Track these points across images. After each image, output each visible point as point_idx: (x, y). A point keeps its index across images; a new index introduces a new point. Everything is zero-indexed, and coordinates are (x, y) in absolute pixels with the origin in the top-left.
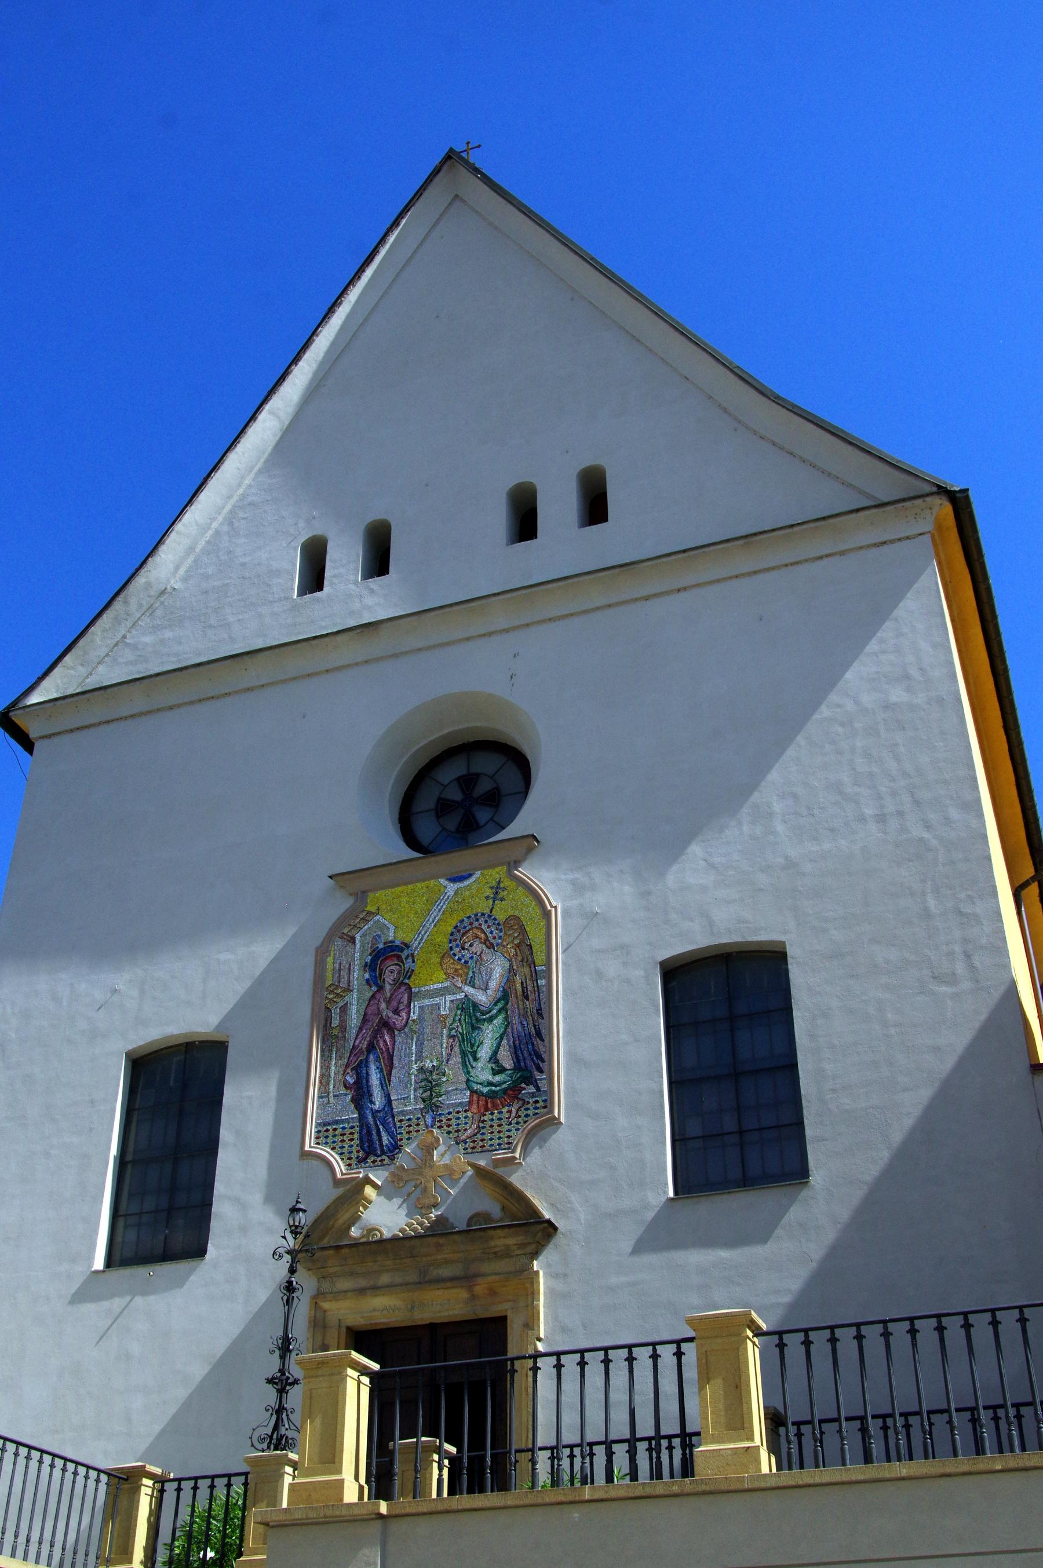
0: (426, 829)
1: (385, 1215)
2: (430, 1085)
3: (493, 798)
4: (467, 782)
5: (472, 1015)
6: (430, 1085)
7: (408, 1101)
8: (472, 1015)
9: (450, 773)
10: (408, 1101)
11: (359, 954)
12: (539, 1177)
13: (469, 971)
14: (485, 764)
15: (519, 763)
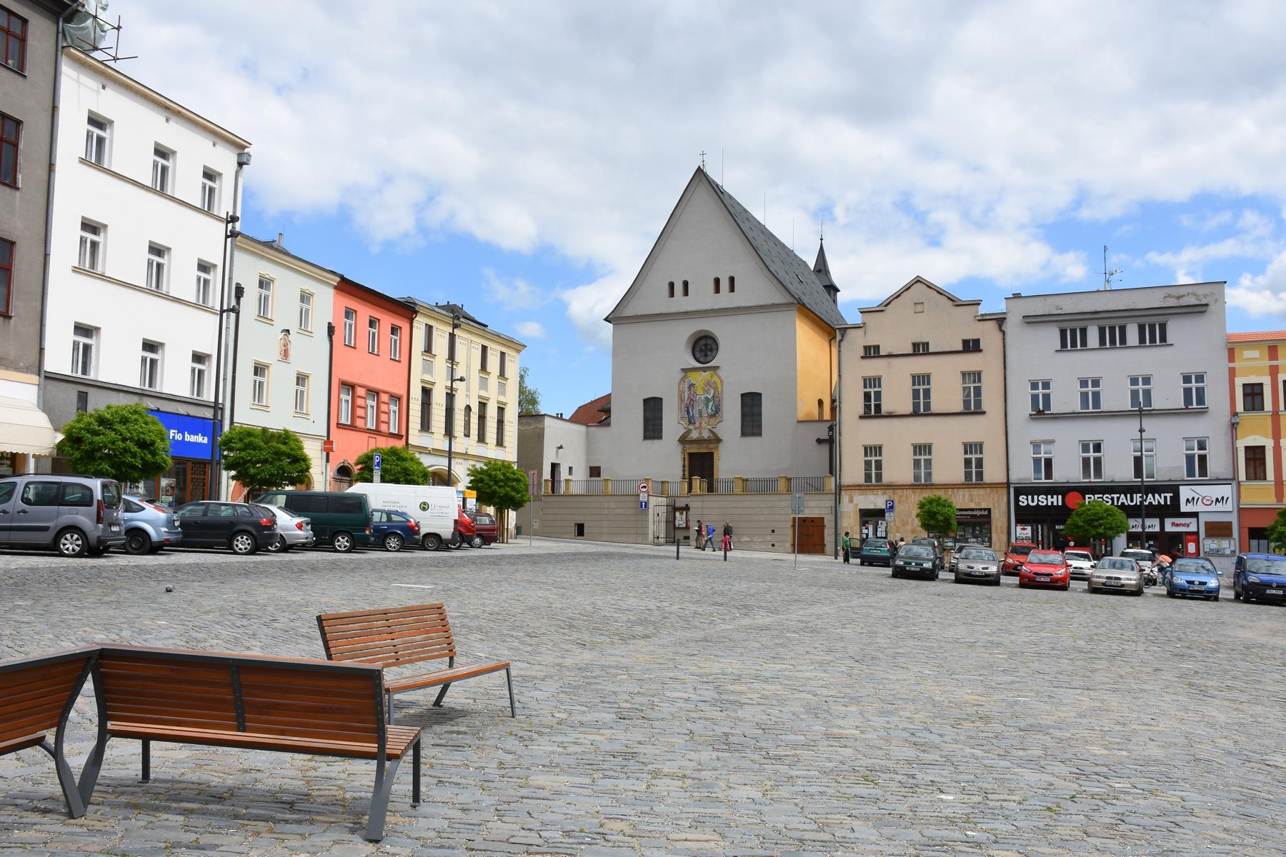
0: (698, 355)
1: (694, 435)
2: (700, 412)
3: (711, 350)
4: (706, 345)
5: (708, 400)
6: (700, 412)
7: (697, 415)
8: (708, 400)
9: (702, 342)
10: (697, 415)
11: (687, 385)
12: (721, 431)
13: (707, 392)
14: (710, 342)
15: (715, 341)
